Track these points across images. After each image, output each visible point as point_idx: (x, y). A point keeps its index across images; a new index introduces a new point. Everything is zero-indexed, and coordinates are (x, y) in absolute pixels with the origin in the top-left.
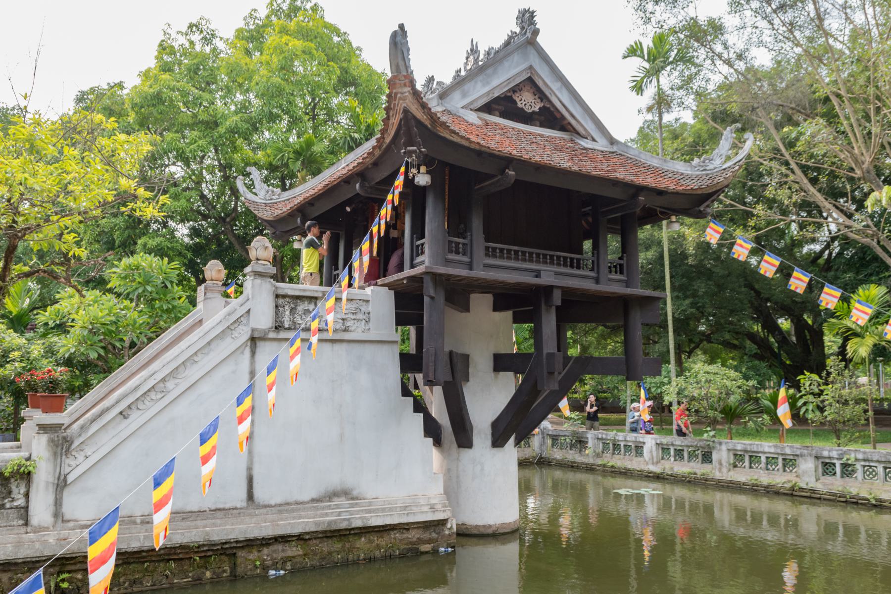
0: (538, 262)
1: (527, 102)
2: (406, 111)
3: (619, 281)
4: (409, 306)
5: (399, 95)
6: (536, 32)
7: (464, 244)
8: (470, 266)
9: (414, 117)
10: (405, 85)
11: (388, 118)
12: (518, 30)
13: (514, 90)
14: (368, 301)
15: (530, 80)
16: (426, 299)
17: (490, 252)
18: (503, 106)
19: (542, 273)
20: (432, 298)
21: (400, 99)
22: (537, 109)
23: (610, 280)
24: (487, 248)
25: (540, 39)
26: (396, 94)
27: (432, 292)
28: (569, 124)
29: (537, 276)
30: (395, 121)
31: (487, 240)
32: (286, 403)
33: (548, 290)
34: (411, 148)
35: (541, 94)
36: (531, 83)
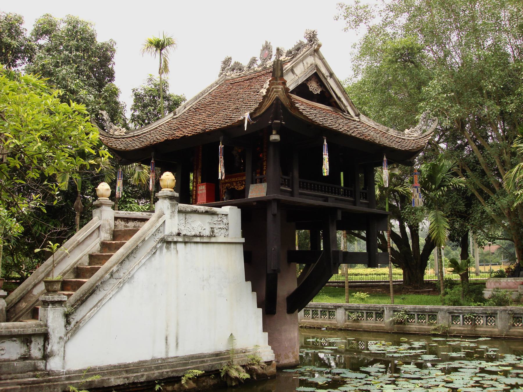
0: (325, 192)
1: (314, 88)
2: (277, 99)
3: (365, 203)
4: (253, 220)
5: (274, 90)
6: (319, 46)
7: (288, 180)
8: (292, 194)
9: (282, 104)
10: (279, 84)
11: (263, 102)
12: (306, 41)
13: (307, 80)
14: (226, 215)
15: (316, 74)
16: (270, 218)
17: (302, 186)
18: (302, 90)
19: (329, 199)
20: (274, 215)
21: (275, 92)
22: (319, 92)
23: (362, 203)
24: (300, 182)
25: (321, 50)
26: (273, 89)
27: (275, 211)
28: (335, 102)
29: (325, 201)
30: (268, 104)
31: (300, 177)
32: (180, 286)
33: (335, 210)
34: (277, 121)
35: (321, 84)
36: (317, 77)
